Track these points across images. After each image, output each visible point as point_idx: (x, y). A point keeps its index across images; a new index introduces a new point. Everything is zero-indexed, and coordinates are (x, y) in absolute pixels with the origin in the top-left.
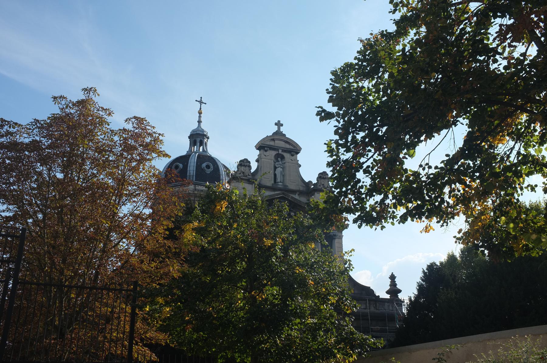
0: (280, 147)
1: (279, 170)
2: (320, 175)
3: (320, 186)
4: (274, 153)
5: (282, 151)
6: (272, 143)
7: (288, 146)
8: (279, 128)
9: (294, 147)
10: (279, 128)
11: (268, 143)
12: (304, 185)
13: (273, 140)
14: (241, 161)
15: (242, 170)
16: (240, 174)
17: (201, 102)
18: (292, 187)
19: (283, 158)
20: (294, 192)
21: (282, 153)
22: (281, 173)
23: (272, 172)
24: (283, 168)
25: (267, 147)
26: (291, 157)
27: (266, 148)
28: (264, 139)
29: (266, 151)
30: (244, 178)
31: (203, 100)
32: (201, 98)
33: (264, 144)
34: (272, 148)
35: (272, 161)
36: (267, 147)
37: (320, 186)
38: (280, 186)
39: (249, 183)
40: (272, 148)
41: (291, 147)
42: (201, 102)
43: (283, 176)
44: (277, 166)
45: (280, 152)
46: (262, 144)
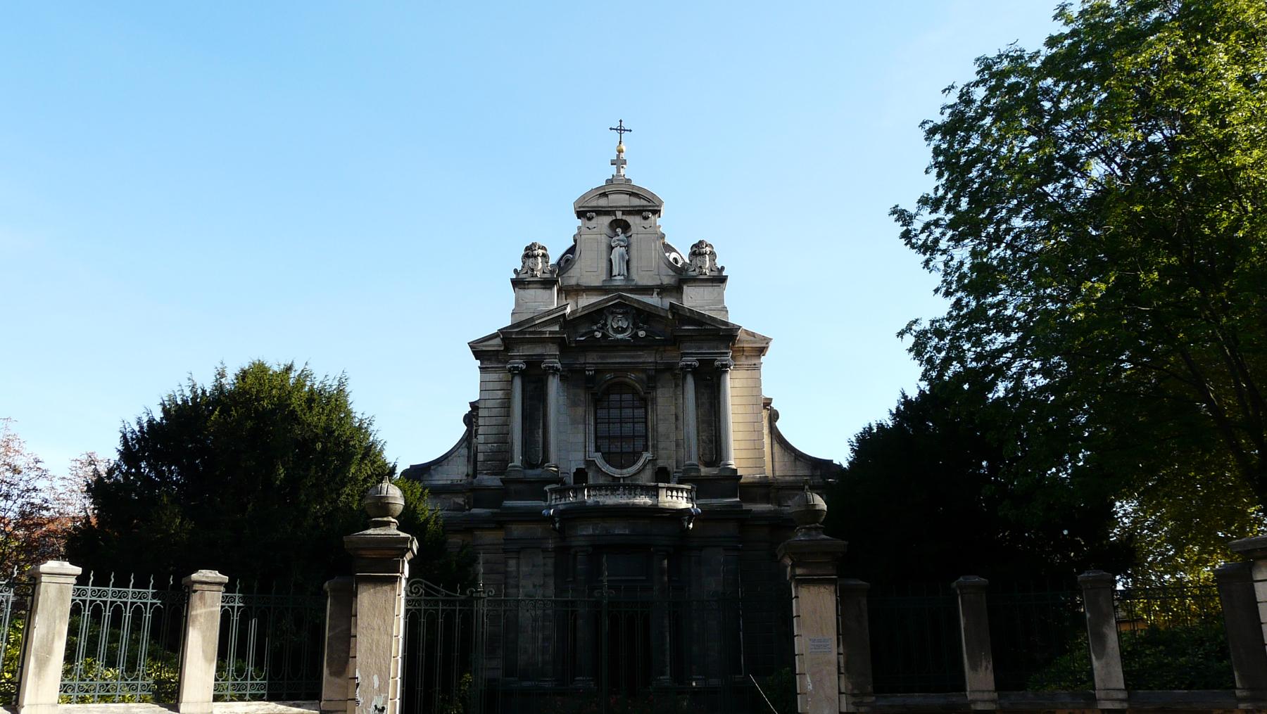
0: (616, 207)
1: (618, 251)
2: (694, 249)
3: (694, 270)
4: (606, 220)
5: (623, 214)
6: (603, 202)
7: (636, 202)
8: (618, 171)
9: (649, 201)
10: (618, 171)
11: (594, 203)
12: (673, 273)
13: (604, 195)
14: (527, 248)
15: (530, 265)
16: (527, 273)
17: (621, 130)
18: (641, 278)
19: (626, 227)
20: (647, 290)
21: (624, 218)
22: (622, 256)
23: (604, 255)
24: (628, 247)
25: (589, 211)
26: (643, 221)
27: (588, 214)
28: (583, 197)
29: (590, 219)
30: (532, 279)
31: (625, 125)
32: (621, 121)
33: (583, 207)
34: (600, 212)
35: (604, 237)
36: (589, 211)
37: (694, 270)
38: (618, 283)
39: (543, 288)
40: (600, 212)
41: (644, 203)
42: (621, 130)
43: (628, 262)
44: (613, 245)
45: (619, 215)
46: (580, 207)
